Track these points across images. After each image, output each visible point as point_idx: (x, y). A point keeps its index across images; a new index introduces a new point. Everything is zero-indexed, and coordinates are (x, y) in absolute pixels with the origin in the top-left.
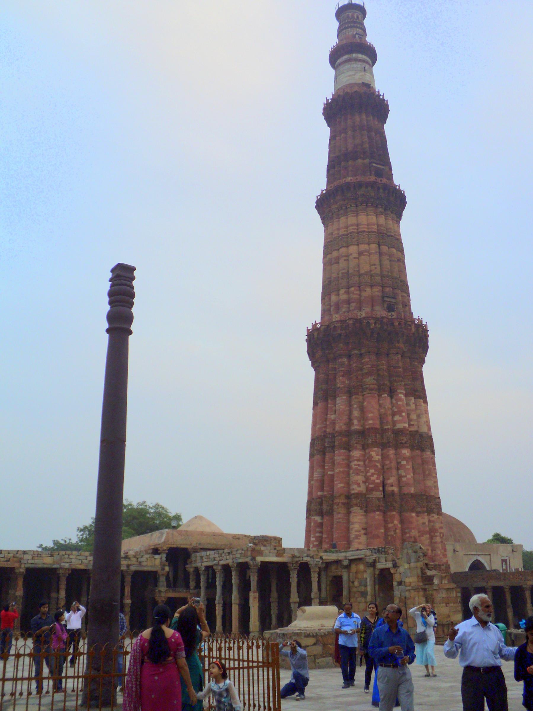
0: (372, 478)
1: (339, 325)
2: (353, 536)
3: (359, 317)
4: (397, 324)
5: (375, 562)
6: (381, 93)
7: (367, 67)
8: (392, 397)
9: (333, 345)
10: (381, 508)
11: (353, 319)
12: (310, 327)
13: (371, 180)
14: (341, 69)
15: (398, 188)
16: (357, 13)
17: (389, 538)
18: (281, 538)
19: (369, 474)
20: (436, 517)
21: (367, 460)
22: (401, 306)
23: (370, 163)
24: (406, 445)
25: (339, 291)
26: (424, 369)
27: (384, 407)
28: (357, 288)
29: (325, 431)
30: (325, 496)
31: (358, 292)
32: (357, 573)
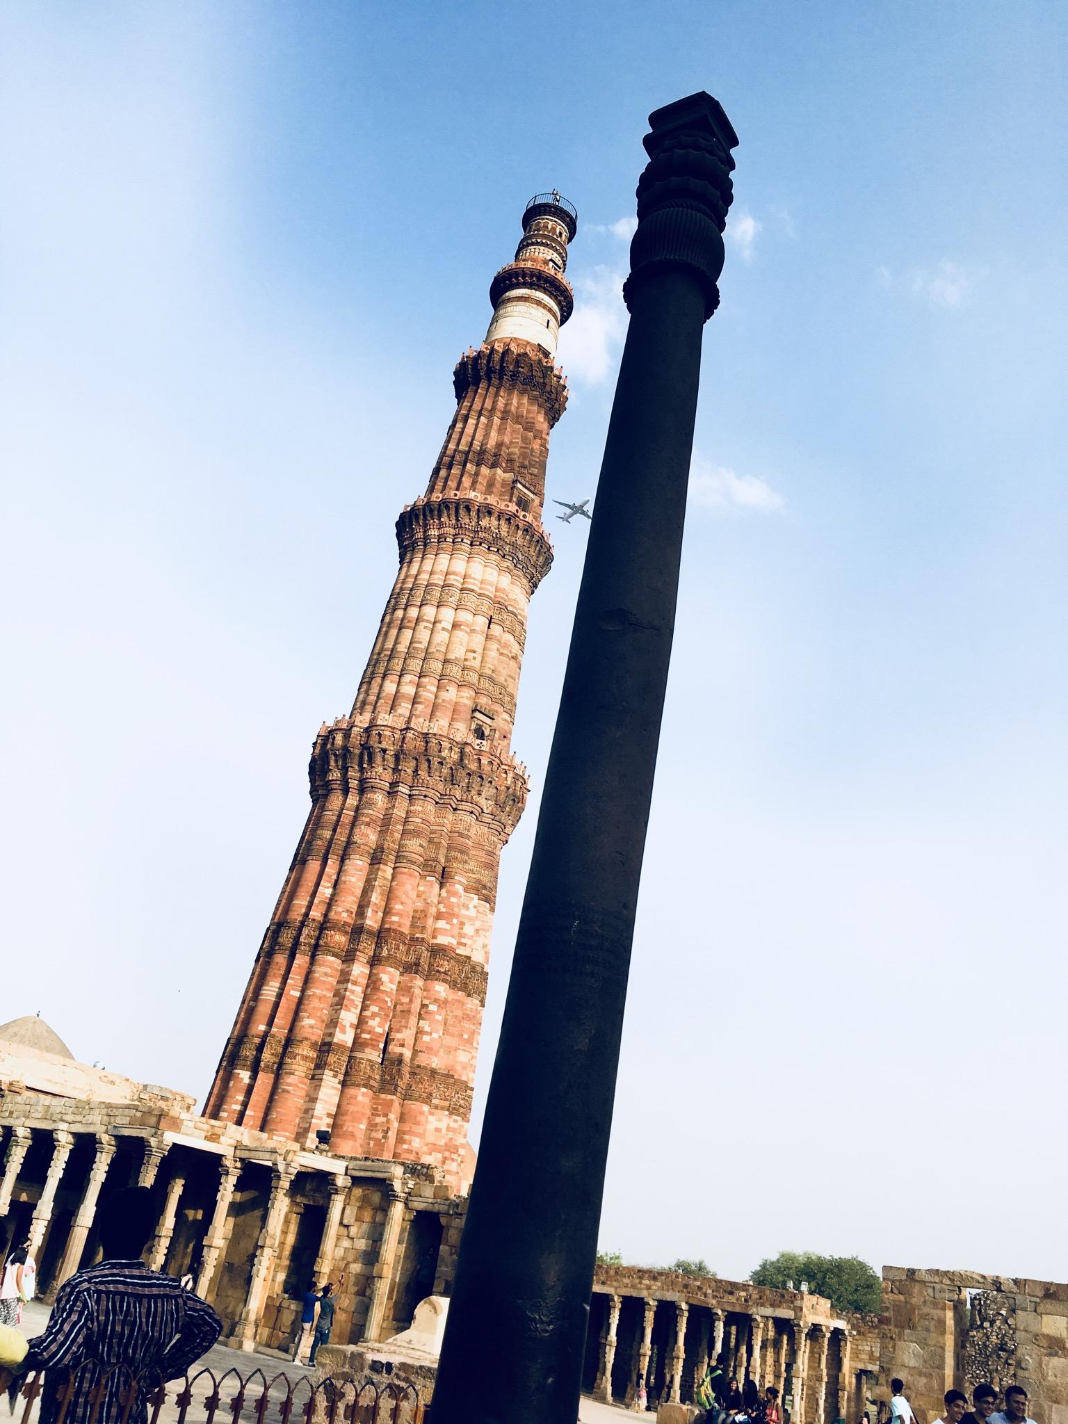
1: (388, 733)
7: (553, 323)
8: (442, 885)
10: (372, 1082)
16: (561, 227)
17: (372, 1143)
19: (367, 1013)
21: (372, 984)
23: (515, 482)
29: (306, 915)
30: (273, 1036)
31: (435, 690)
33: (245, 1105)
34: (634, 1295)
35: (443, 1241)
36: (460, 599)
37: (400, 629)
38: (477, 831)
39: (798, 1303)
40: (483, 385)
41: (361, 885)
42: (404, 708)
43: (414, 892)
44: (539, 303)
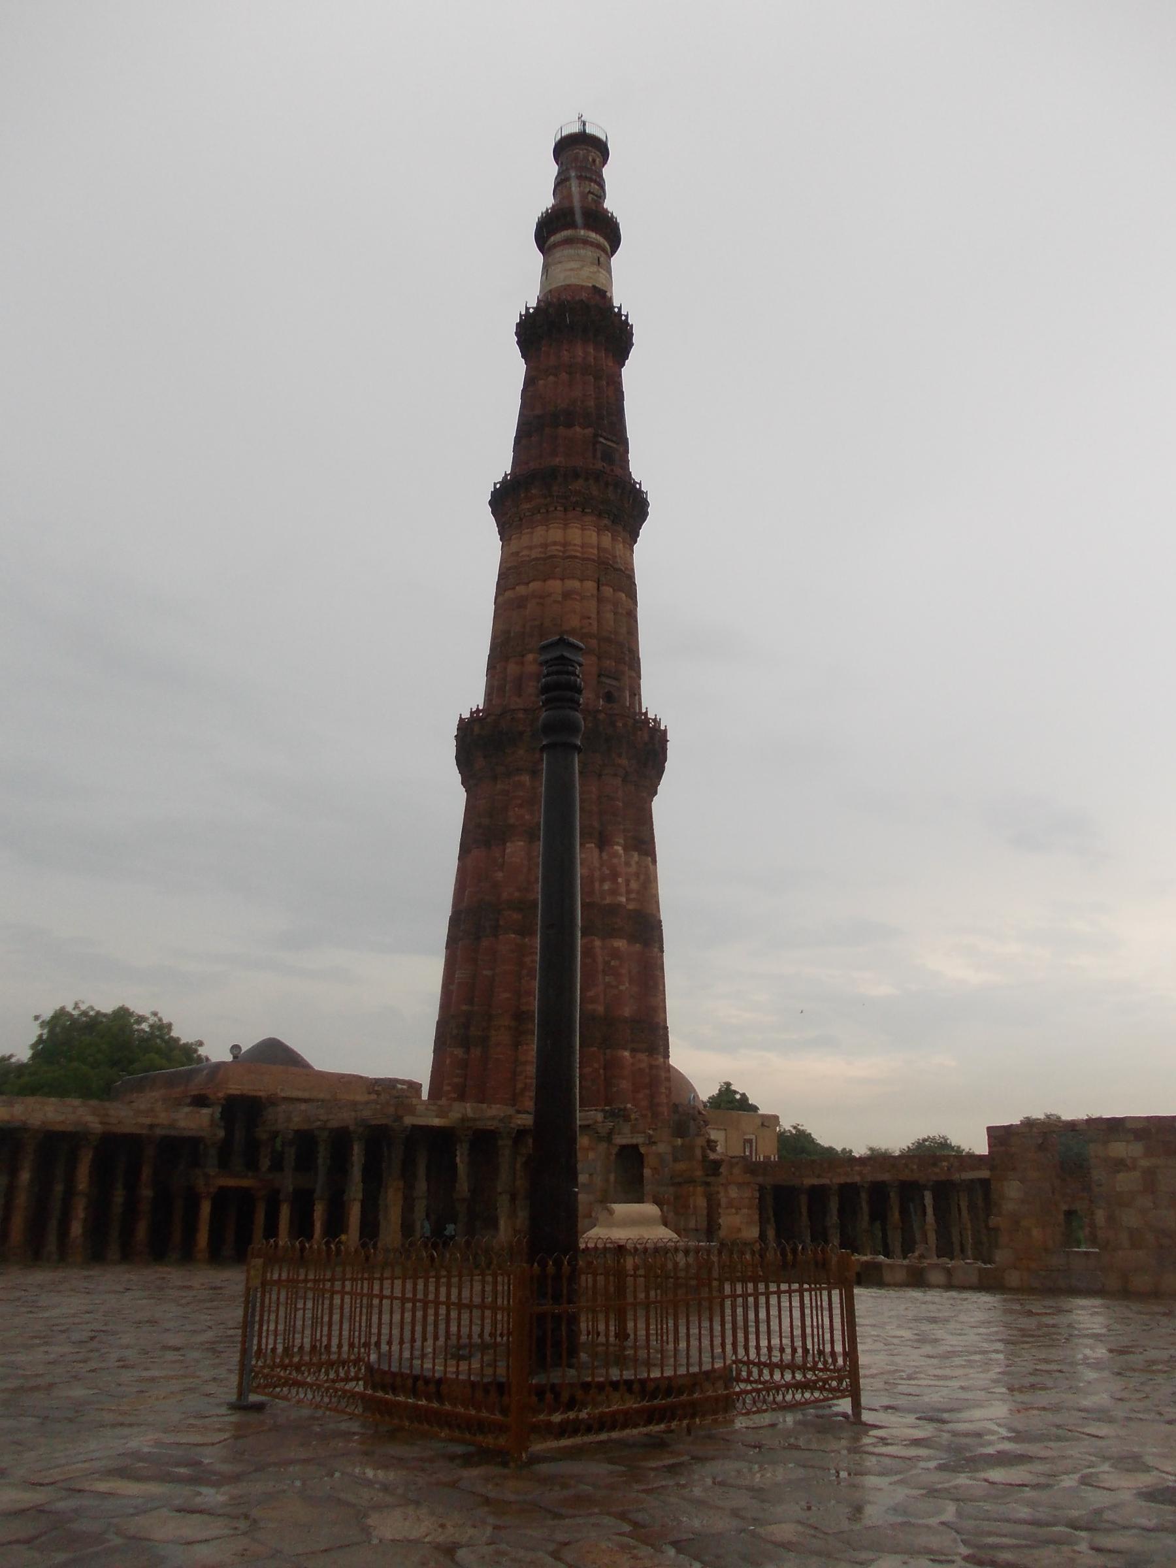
2: (520, 1086)
5: (611, 1133)
6: (624, 312)
16: (594, 154)
23: (596, 435)
34: (849, 1181)
35: (645, 1164)
44: (586, 242)
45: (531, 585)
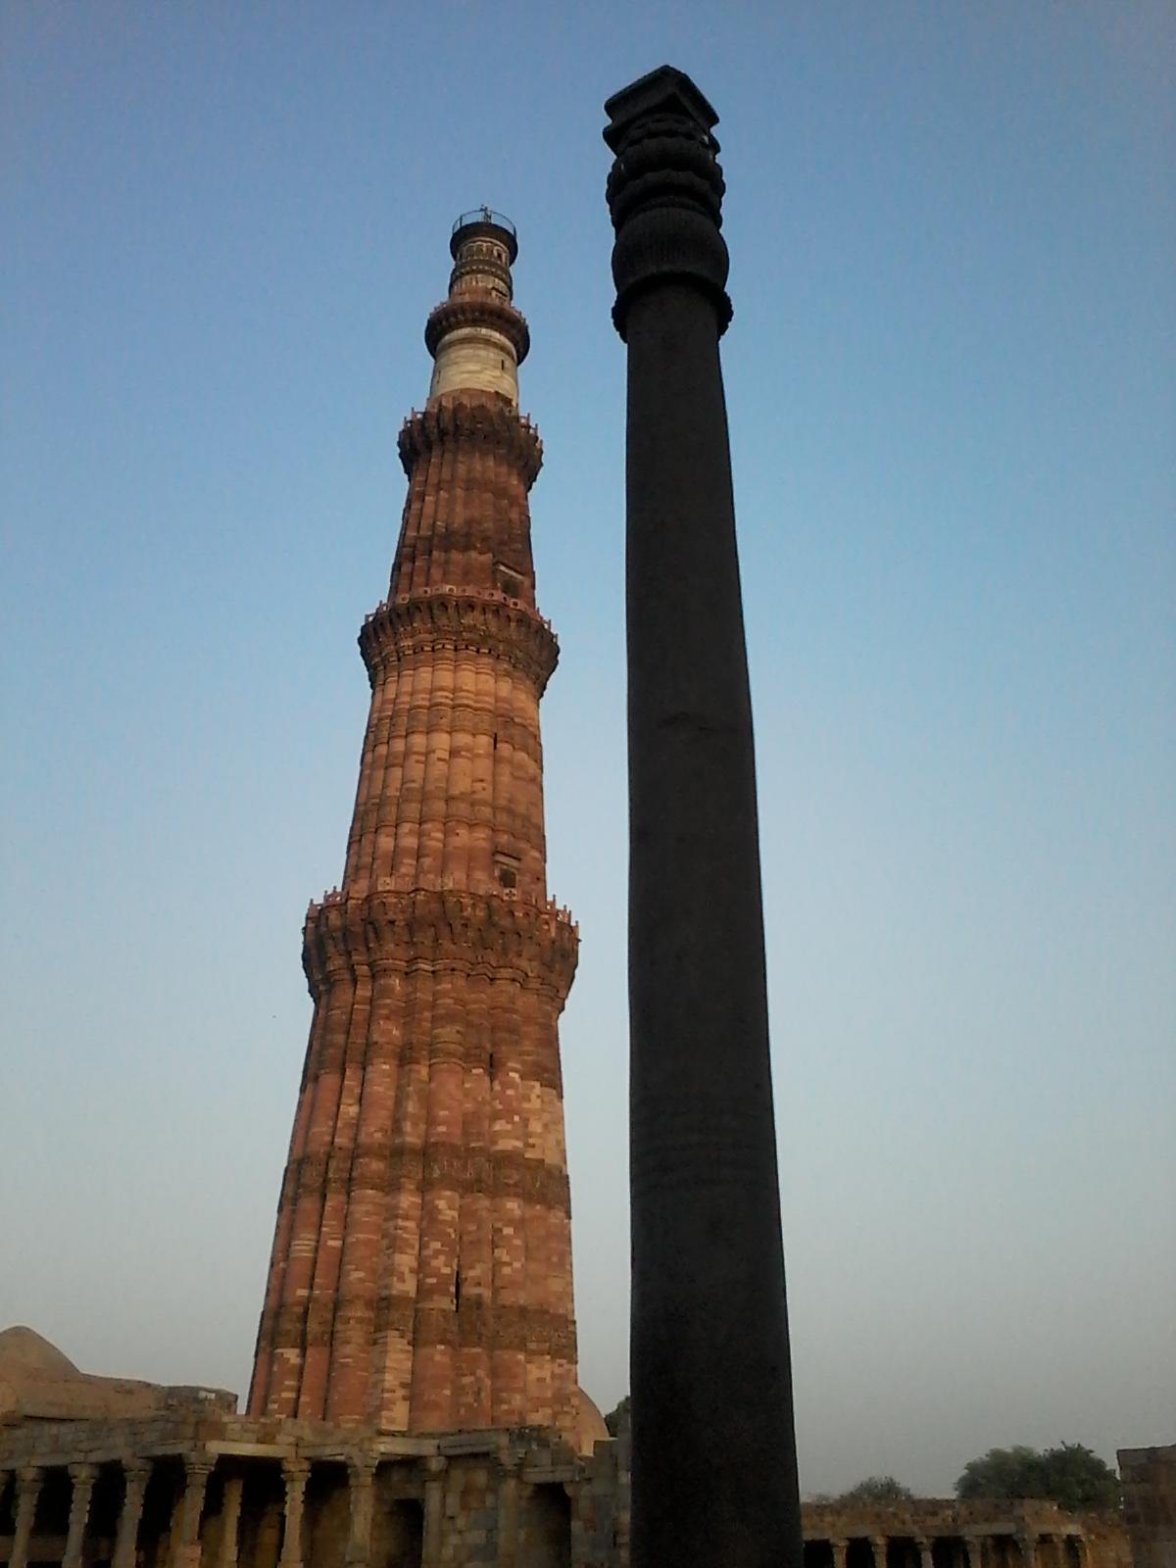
0: (435, 1263)
3: (438, 889)
4: (521, 915)
5: (521, 1465)
7: (508, 363)
9: (371, 945)
10: (449, 1336)
11: (426, 891)
12: (319, 900)
13: (495, 598)
14: (453, 356)
15: (546, 626)
16: (499, 248)
17: (462, 1411)
18: (236, 1397)
19: (425, 1253)
20: (567, 1366)
21: (428, 1213)
22: (527, 879)
24: (517, 1190)
25: (396, 826)
26: (560, 1022)
27: (475, 1099)
28: (440, 826)
31: (440, 835)
32: (465, 1493)
33: (299, 1391)
36: (453, 720)
37: (386, 768)
38: (527, 1002)
39: (1018, 1512)
40: (436, 452)
41: (392, 1093)
42: (407, 866)
43: (459, 1092)
44: (487, 342)
45: (408, 739)
